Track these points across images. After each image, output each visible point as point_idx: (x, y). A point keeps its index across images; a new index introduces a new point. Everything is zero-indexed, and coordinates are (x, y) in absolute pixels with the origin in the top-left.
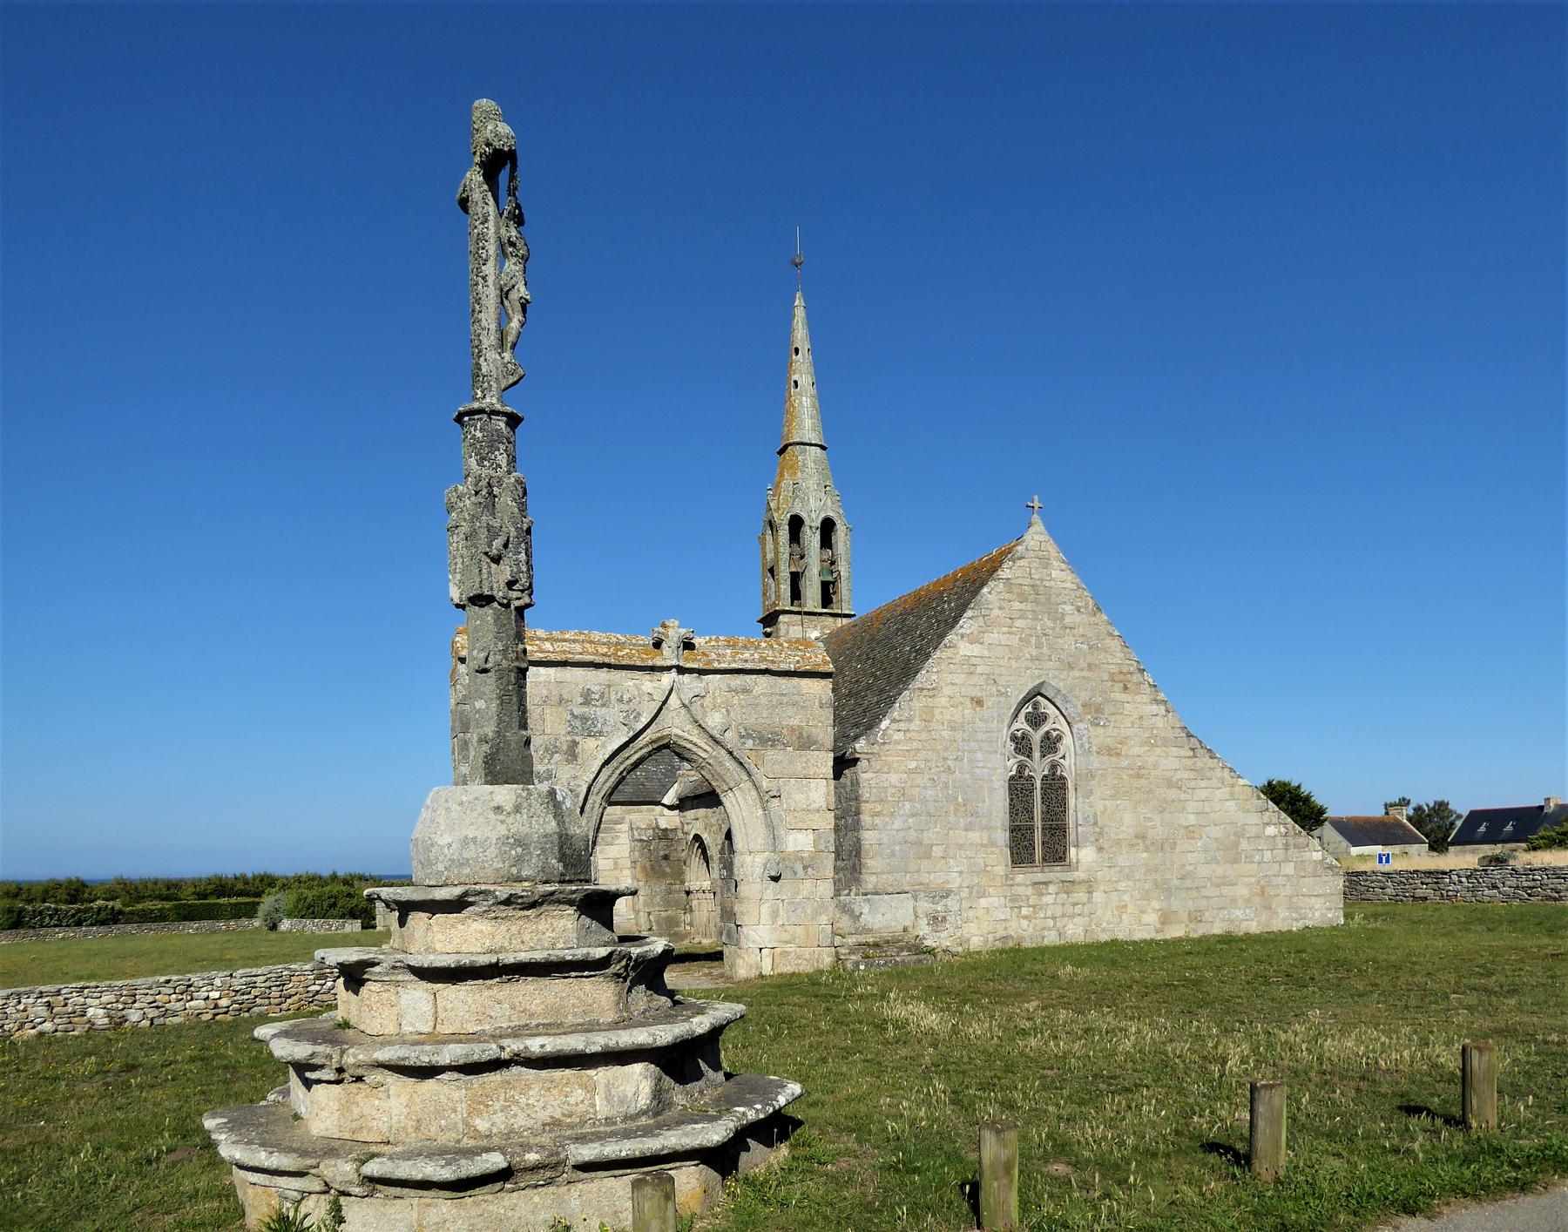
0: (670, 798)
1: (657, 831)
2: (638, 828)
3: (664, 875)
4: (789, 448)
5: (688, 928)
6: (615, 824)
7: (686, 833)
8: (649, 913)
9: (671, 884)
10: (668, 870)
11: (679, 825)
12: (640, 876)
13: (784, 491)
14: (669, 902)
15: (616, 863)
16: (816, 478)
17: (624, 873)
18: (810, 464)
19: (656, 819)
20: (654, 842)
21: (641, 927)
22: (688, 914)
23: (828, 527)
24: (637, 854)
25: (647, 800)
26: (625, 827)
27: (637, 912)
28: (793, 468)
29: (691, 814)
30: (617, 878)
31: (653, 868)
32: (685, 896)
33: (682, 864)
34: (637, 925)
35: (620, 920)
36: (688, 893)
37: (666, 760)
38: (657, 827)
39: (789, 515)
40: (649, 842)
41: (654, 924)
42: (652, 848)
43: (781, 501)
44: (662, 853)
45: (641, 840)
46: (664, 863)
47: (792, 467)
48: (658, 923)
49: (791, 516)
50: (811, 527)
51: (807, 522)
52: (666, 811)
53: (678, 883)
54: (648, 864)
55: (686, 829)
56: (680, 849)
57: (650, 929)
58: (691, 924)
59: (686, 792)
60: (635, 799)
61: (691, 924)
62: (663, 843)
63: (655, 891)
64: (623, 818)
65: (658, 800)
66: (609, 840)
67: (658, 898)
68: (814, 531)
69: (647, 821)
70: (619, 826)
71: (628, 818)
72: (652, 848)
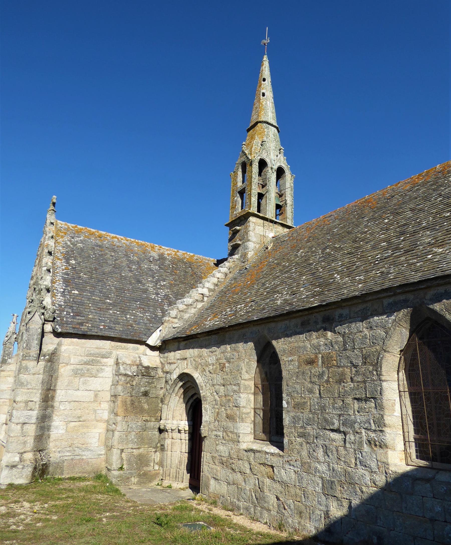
0: (154, 340)
1: (140, 368)
2: (124, 363)
3: (142, 411)
4: (259, 124)
5: (157, 467)
6: (102, 357)
7: (167, 373)
8: (122, 451)
9: (146, 421)
10: (146, 406)
11: (160, 365)
12: (120, 411)
13: (255, 145)
14: (142, 439)
15: (96, 396)
16: (274, 144)
17: (102, 406)
18: (271, 136)
19: (139, 357)
20: (137, 378)
21: (111, 465)
22: (158, 453)
23: (280, 172)
24: (120, 388)
25: (135, 338)
26: (111, 361)
27: (109, 448)
28: (262, 134)
29: (173, 356)
30: (95, 411)
31: (132, 403)
32: (157, 433)
33: (159, 401)
34: (107, 461)
35: (90, 456)
36: (161, 431)
37: (151, 310)
38: (141, 364)
39: (259, 158)
40: (133, 377)
41: (125, 462)
42: (134, 383)
43: (253, 150)
44: (143, 389)
45: (126, 375)
46: (143, 399)
47: (260, 134)
48: (129, 461)
49: (260, 159)
50: (272, 168)
51: (269, 165)
52: (148, 351)
53: (153, 419)
54: (129, 398)
55: (167, 368)
56: (159, 386)
57: (121, 468)
58: (161, 464)
59: (169, 336)
60: (124, 337)
61: (161, 464)
62: (145, 380)
63: (131, 428)
64: (111, 353)
65: (144, 340)
66: (94, 372)
67: (132, 436)
68: (274, 171)
69: (132, 358)
70: (105, 360)
71: (114, 352)
72: (134, 383)
